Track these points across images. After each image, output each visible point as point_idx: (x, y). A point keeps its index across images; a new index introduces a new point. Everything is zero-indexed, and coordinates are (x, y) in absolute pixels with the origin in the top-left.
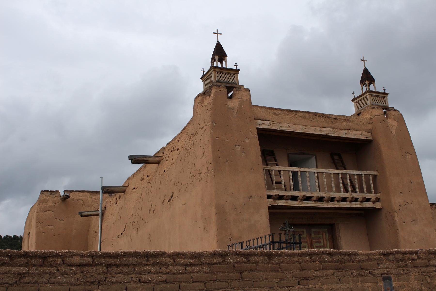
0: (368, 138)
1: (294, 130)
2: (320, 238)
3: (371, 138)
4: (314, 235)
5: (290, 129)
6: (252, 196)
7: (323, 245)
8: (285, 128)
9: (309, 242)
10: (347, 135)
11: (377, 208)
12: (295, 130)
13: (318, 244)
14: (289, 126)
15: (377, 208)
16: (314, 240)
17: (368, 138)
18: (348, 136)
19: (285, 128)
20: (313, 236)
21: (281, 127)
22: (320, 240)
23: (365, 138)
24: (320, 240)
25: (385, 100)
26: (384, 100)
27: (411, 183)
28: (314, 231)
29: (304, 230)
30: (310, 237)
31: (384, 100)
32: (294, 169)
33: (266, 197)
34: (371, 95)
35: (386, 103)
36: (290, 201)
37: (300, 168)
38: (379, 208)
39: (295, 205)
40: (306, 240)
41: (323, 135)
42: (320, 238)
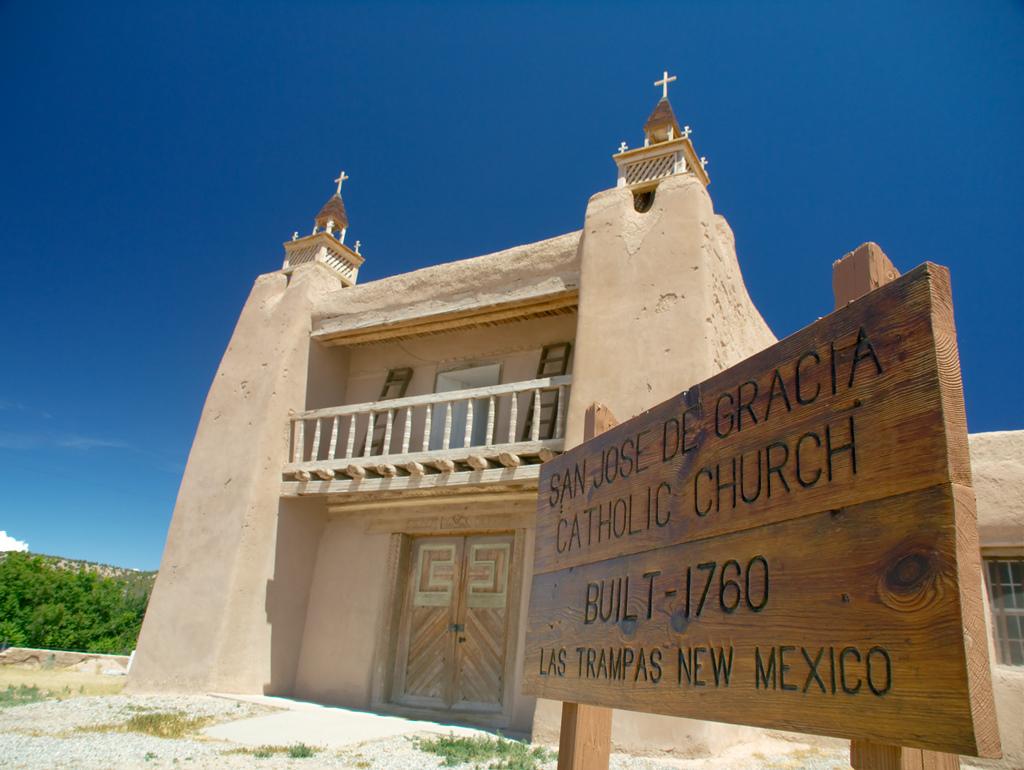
2: (486, 568)
4: (476, 560)
5: (377, 319)
7: (490, 584)
9: (457, 577)
13: (479, 585)
16: (472, 574)
20: (472, 563)
22: (487, 572)
24: (487, 572)
27: (650, 387)
28: (477, 551)
29: (453, 547)
30: (463, 562)
40: (451, 573)
42: (486, 568)
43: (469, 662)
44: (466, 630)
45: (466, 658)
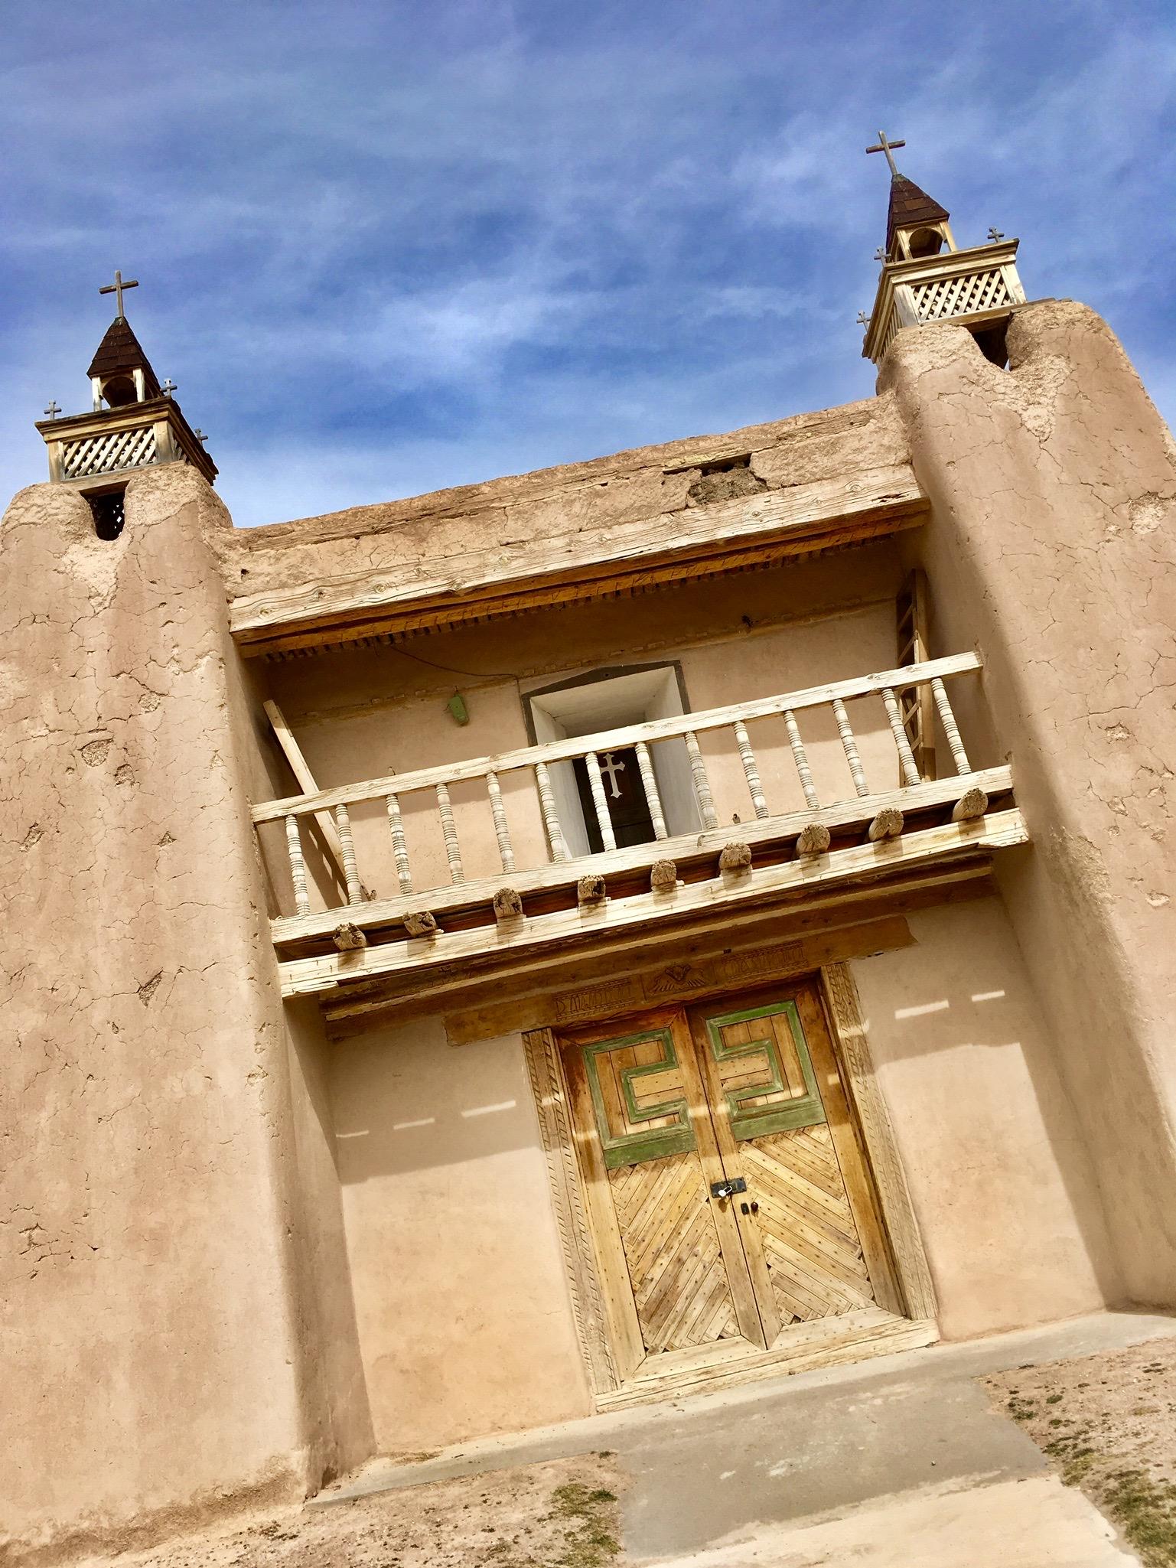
0: (897, 496)
1: (452, 583)
3: (913, 494)
5: (429, 583)
6: (158, 976)
8: (402, 590)
10: (766, 519)
11: (998, 848)
12: (459, 581)
14: (425, 572)
15: (998, 844)
17: (897, 496)
18: (772, 524)
19: (402, 590)
21: (378, 588)
23: (878, 504)
25: (1001, 281)
26: (995, 281)
31: (995, 281)
32: (457, 771)
33: (274, 954)
34: (907, 283)
35: (1007, 297)
36: (442, 938)
37: (494, 758)
38: (1009, 843)
39: (471, 949)
41: (622, 561)
43: (778, 1245)
44: (750, 1187)
45: (769, 1240)
